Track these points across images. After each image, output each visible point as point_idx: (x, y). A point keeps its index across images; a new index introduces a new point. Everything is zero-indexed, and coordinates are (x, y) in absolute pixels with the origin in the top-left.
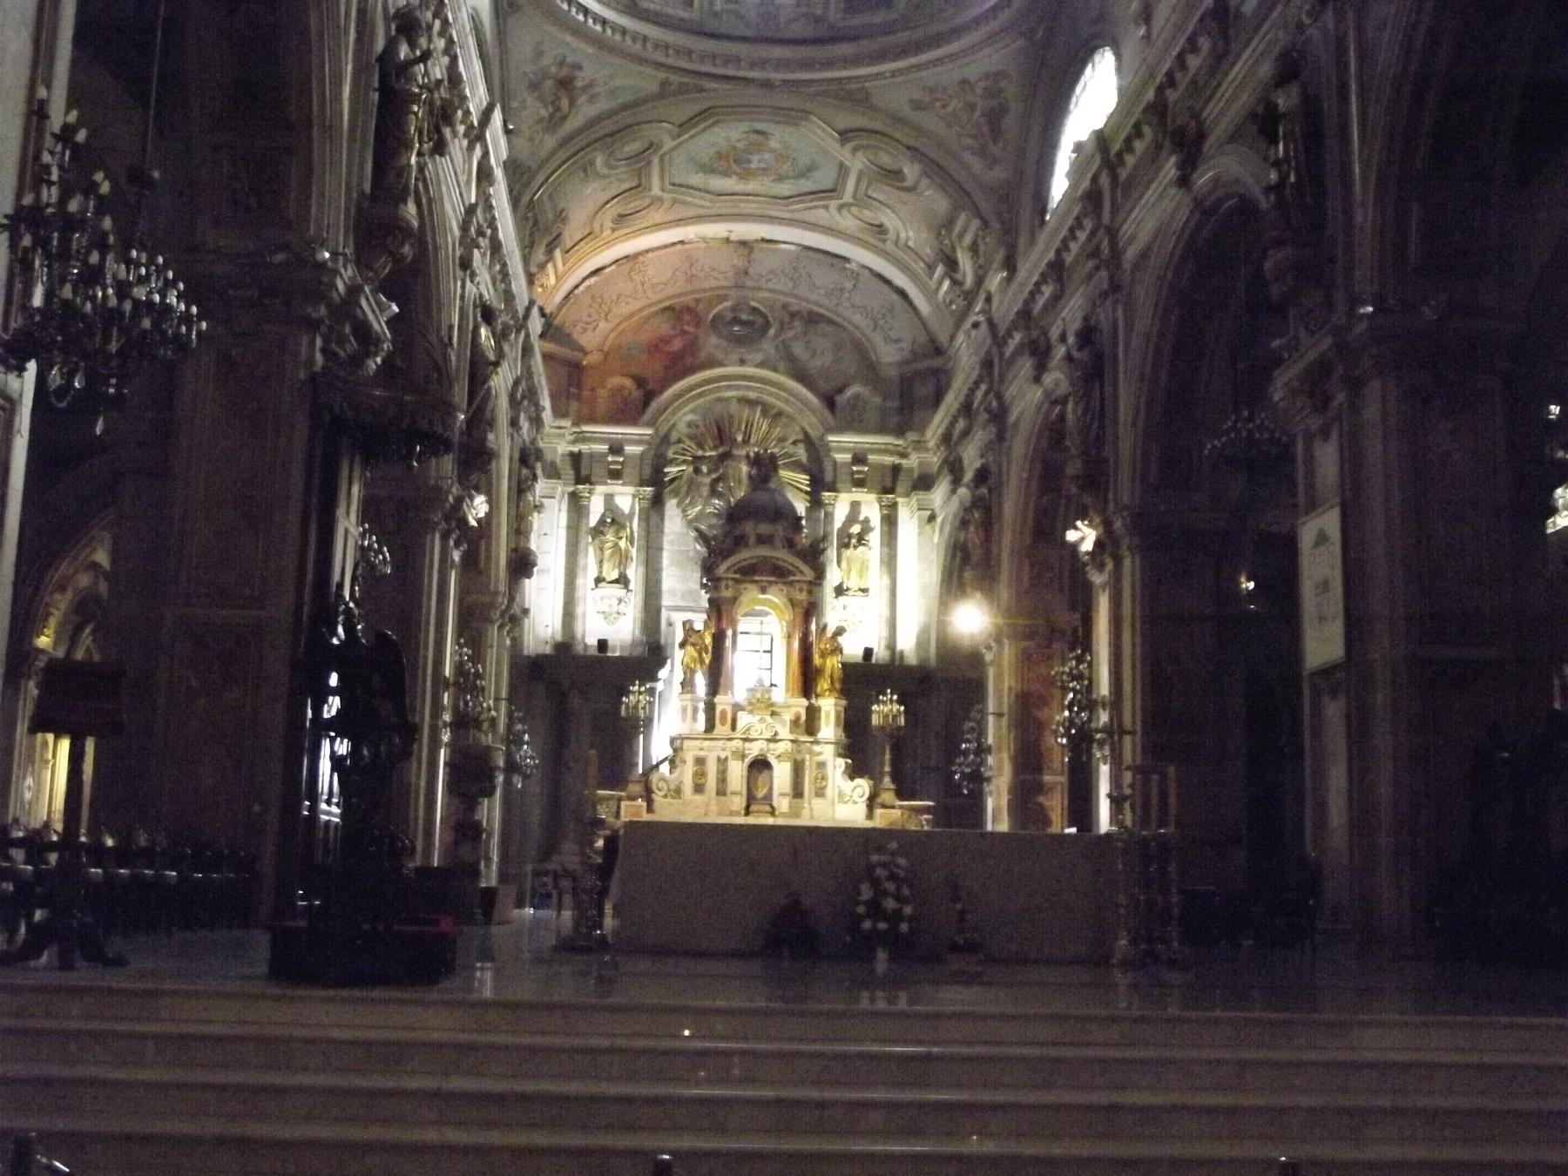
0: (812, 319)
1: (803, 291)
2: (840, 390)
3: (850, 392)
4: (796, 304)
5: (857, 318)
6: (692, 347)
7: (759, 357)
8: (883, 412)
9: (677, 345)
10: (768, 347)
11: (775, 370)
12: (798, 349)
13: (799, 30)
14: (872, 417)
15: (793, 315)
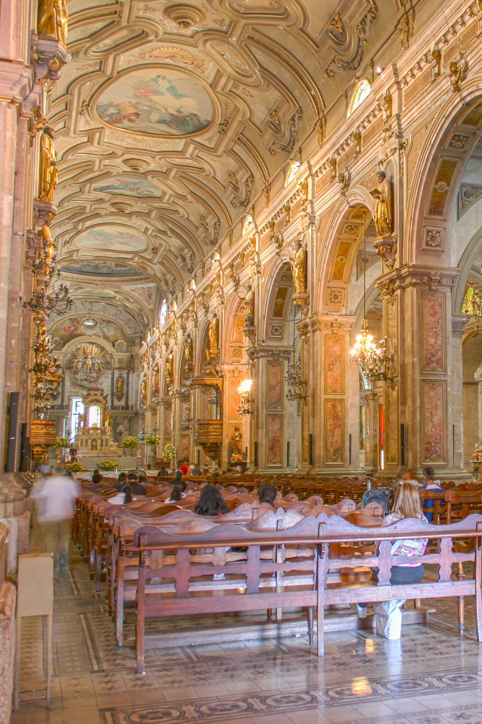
0: (109, 322)
1: (106, 315)
2: (116, 341)
3: (118, 341)
4: (105, 318)
5: (121, 322)
6: (76, 329)
7: (95, 332)
8: (127, 346)
9: (72, 328)
10: (97, 330)
11: (99, 336)
12: (105, 330)
13: (104, 270)
14: (124, 348)
15: (104, 321)
